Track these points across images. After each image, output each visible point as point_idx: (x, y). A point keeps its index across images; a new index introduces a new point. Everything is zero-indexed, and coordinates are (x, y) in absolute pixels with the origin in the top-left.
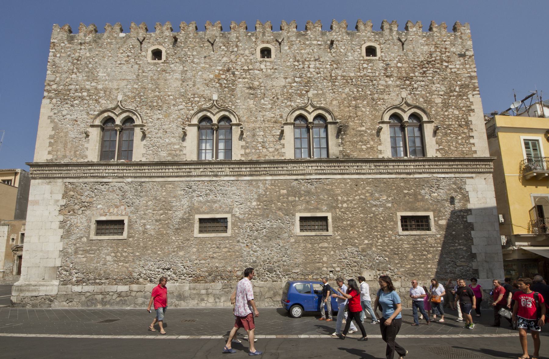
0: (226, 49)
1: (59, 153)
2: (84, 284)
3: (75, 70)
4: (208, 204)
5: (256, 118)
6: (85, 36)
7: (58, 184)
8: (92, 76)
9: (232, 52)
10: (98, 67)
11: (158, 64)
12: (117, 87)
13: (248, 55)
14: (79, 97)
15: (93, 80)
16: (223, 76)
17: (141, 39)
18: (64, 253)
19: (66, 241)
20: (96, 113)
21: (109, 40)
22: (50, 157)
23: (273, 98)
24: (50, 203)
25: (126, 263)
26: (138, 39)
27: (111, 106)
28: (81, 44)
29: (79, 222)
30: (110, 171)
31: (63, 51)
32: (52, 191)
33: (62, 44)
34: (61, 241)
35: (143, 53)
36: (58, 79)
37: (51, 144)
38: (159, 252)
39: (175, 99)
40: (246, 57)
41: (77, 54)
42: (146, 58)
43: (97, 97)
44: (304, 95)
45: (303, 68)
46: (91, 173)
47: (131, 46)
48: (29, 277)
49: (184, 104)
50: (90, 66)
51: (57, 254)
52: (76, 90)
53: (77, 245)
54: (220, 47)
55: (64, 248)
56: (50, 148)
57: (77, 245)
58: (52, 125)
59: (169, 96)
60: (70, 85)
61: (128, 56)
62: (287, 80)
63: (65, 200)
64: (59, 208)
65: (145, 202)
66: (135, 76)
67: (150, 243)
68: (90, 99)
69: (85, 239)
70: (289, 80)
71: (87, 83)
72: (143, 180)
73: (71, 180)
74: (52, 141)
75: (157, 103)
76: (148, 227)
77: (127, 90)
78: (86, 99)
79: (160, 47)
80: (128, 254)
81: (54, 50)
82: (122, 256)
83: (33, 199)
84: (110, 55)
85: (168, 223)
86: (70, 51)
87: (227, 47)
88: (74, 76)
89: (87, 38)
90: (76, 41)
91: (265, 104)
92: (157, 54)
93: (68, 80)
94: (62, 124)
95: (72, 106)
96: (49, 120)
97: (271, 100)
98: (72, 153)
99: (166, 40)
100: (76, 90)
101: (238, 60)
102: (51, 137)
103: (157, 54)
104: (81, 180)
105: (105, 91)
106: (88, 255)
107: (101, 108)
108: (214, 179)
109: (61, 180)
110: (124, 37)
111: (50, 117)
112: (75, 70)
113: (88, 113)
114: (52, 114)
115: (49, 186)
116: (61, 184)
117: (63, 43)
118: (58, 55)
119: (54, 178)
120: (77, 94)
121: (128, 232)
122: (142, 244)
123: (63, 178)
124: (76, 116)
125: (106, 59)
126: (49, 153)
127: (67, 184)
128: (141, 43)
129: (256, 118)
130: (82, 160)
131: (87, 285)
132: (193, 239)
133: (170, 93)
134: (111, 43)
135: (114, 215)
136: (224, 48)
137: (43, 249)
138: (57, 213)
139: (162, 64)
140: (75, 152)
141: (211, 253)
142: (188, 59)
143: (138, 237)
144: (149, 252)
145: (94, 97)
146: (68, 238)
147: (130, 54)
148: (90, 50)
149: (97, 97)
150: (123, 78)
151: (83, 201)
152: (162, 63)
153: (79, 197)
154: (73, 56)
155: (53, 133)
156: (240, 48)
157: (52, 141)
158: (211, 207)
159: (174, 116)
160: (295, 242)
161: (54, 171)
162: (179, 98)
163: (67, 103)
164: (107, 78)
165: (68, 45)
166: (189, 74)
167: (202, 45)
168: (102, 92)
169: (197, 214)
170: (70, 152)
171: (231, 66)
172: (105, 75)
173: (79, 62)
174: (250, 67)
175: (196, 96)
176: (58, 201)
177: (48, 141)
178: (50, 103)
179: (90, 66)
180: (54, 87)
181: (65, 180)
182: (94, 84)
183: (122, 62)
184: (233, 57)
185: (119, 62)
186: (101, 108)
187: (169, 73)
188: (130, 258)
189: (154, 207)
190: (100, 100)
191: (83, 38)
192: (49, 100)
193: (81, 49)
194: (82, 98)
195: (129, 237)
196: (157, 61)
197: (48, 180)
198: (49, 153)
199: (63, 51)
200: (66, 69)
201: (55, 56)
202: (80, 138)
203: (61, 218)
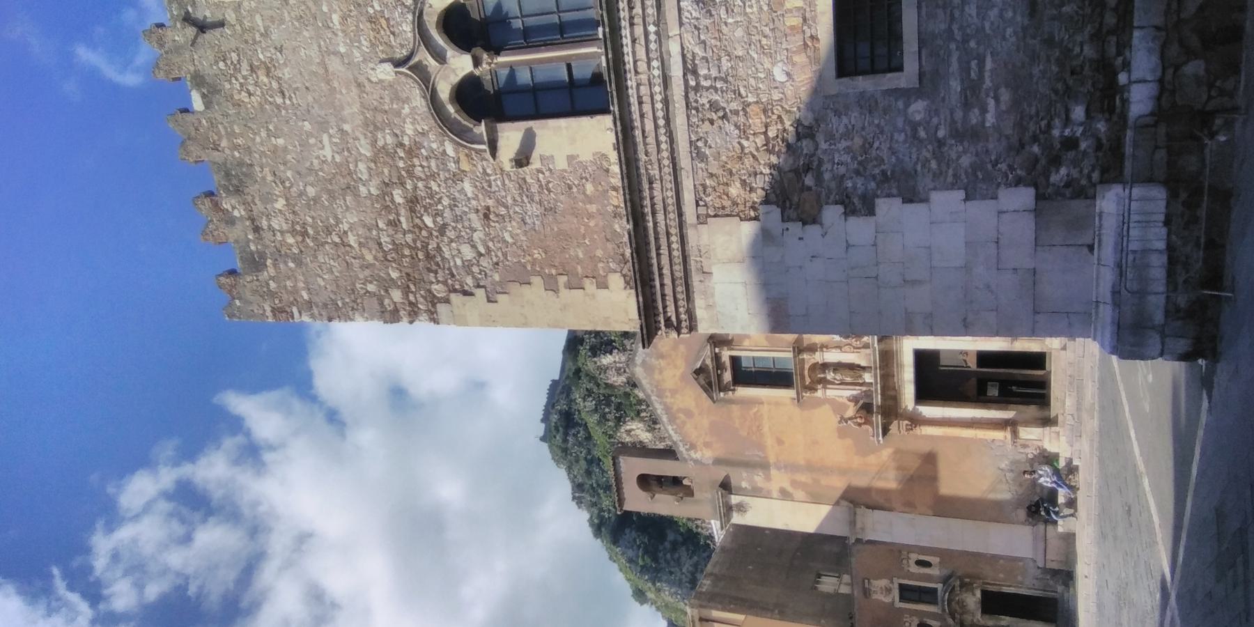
1: (599, 253)
2: (1122, 78)
6: (231, 221)
7: (705, 239)
8: (342, 183)
10: (308, 164)
12: (355, 91)
14: (412, 210)
15: (350, 174)
17: (191, 31)
18: (977, 185)
19: (924, 182)
22: (616, 281)
26: (194, 43)
27: (418, 101)
28: (257, 229)
29: (844, 144)
30: (641, 53)
33: (273, 285)
34: (926, 200)
41: (290, 240)
46: (656, 127)
50: (311, 191)
51: (981, 210)
52: (394, 224)
53: (941, 134)
57: (941, 134)
58: (514, 288)
60: (380, 244)
61: (253, 69)
64: (795, 228)
68: (411, 174)
69: (918, 109)
71: (363, 190)
73: (688, 197)
74: (562, 280)
77: (356, 53)
78: (415, 188)
84: (264, 134)
86: (286, 263)
88: (352, 239)
89: (236, 213)
90: (253, 248)
93: (369, 258)
94: (505, 255)
95: (442, 229)
98: (593, 208)
100: (394, 224)
102: (551, 286)
104: (685, 161)
105: (376, 128)
106: (988, 83)
107: (432, 136)
109: (691, 234)
110: (204, 96)
113: (457, 177)
114: (480, 293)
115: (714, 270)
120: (403, 219)
123: (681, 225)
124: (473, 216)
125: (280, 141)
126: (603, 285)
127: (702, 210)
130: (616, 169)
131: (1127, 66)
134: (231, 135)
138: (813, 230)
140: (589, 200)
145: (401, 164)
148: (268, 198)
150: (321, 71)
151: (760, 140)
153: (748, 162)
155: (537, 280)
161: (664, 262)
163: (439, 249)
165: (272, 271)
170: (590, 216)
172: (325, 138)
173: (311, 231)
177: (564, 292)
178: (447, 301)
179: (311, 191)
180: (397, 295)
185: (279, 100)
186: (432, 136)
191: (239, 226)
192: (438, 305)
194: (413, 202)
197: (695, 279)
198: (603, 285)
199: (289, 283)
202: (541, 186)
203: (832, 213)
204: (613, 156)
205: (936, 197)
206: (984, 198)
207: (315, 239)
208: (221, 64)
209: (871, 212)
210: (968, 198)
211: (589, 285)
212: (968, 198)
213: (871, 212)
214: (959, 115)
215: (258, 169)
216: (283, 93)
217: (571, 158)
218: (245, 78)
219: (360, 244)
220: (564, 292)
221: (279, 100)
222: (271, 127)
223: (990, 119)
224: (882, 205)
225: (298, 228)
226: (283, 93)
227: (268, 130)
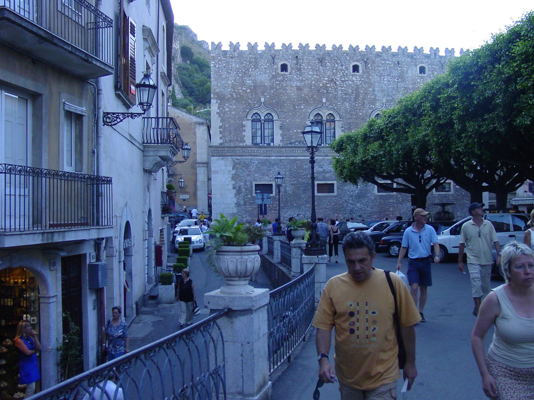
11: (285, 75)
16: (328, 85)
18: (238, 205)
19: (238, 196)
22: (221, 141)
28: (232, 57)
33: (219, 58)
35: (275, 67)
51: (233, 205)
56: (221, 135)
58: (220, 118)
61: (265, 68)
72: (282, 158)
74: (221, 130)
79: (286, 63)
82: (273, 207)
87: (330, 64)
92: (284, 68)
102: (220, 127)
104: (243, 157)
108: (326, 158)
111: (217, 113)
118: (217, 66)
126: (221, 138)
135: (266, 180)
136: (328, 64)
140: (237, 138)
155: (221, 124)
157: (221, 130)
158: (324, 176)
160: (375, 199)
165: (223, 58)
174: (346, 79)
176: (230, 171)
198: (221, 138)
203: (233, 182)
204: (245, 144)
217: (244, 136)
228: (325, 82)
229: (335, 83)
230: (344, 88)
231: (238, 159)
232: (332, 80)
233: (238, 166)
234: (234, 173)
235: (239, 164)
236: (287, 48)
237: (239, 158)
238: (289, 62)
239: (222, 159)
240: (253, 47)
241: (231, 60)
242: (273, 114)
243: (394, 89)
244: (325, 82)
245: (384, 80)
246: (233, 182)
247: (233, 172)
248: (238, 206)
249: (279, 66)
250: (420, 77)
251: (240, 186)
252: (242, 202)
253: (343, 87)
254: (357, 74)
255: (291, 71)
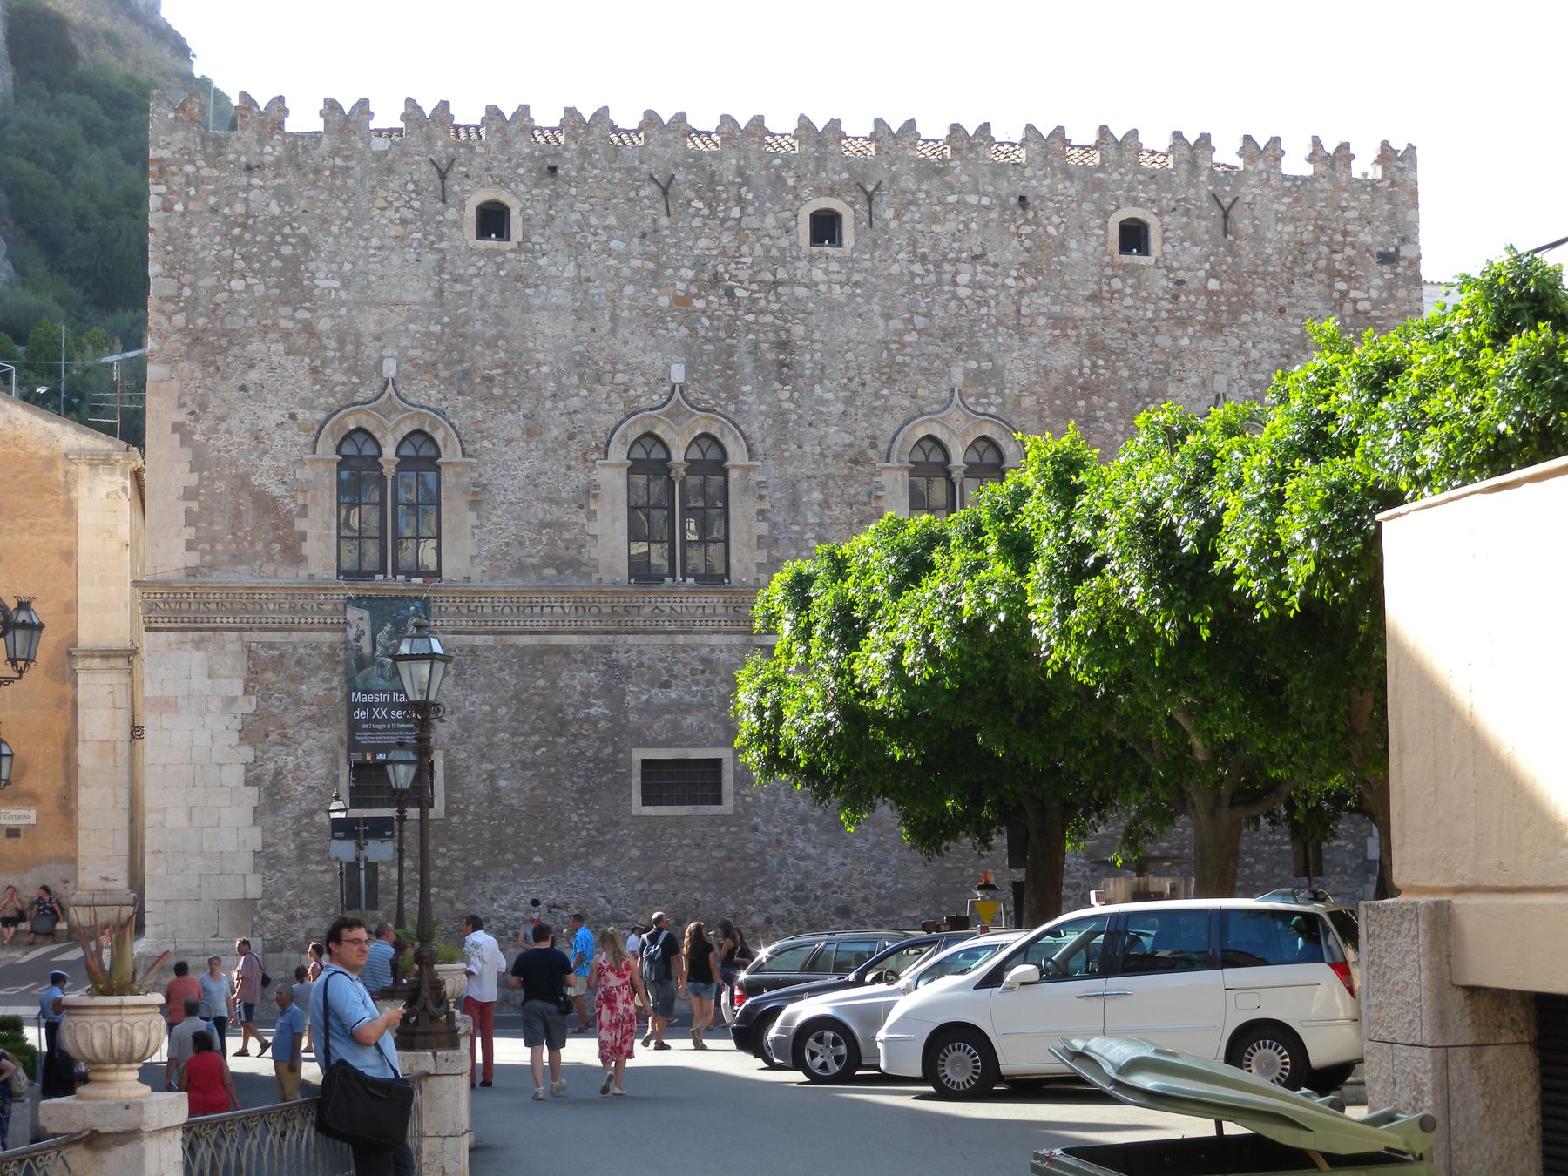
0: (706, 212)
3: (240, 265)
4: (667, 716)
5: (800, 447)
7: (229, 647)
9: (724, 221)
11: (499, 253)
13: (775, 233)
18: (267, 859)
19: (269, 820)
20: (321, 416)
21: (339, 161)
22: (194, 559)
23: (850, 380)
24: (212, 708)
25: (447, 888)
28: (249, 168)
31: (192, 192)
32: (210, 668)
33: (189, 168)
34: (255, 824)
35: (451, 214)
36: (187, 292)
37: (190, 519)
38: (537, 859)
39: (557, 376)
40: (766, 241)
41: (239, 208)
42: (460, 228)
43: (317, 363)
44: (942, 373)
45: (939, 282)
47: (411, 187)
48: (170, 928)
49: (584, 393)
51: (246, 860)
53: (304, 834)
54: (689, 203)
55: (266, 845)
56: (190, 532)
57: (304, 834)
59: (538, 365)
61: (404, 222)
62: (891, 323)
63: (254, 699)
64: (237, 724)
65: (487, 708)
66: (429, 293)
67: (510, 830)
70: (896, 324)
71: (285, 310)
72: (478, 640)
73: (267, 637)
74: (194, 506)
75: (504, 387)
76: (502, 783)
79: (504, 197)
80: (452, 862)
81: (163, 189)
83: (158, 694)
85: (558, 772)
86: (214, 193)
89: (268, 149)
91: (824, 402)
92: (493, 220)
96: (177, 436)
97: (844, 387)
99: (521, 171)
101: (745, 249)
102: (189, 494)
103: (493, 220)
104: (295, 636)
107: (332, 400)
111: (177, 427)
112: (240, 265)
114: (180, 416)
116: (237, 647)
117: (192, 162)
118: (179, 207)
119: (214, 630)
121: (448, 798)
122: (486, 834)
128: (443, 177)
129: (800, 447)
132: (627, 820)
133: (540, 356)
136: (698, 204)
137: (206, 847)
138: (234, 738)
139: (511, 256)
141: (680, 862)
142: (590, 238)
143: (475, 814)
144: (509, 856)
146: (274, 811)
147: (407, 214)
149: (317, 363)
152: (512, 251)
154: (227, 210)
155: (193, 480)
156: (750, 210)
157: (194, 506)
158: (676, 726)
159: (555, 433)
162: (568, 375)
164: (343, 295)
165: (205, 172)
166: (597, 290)
167: (632, 194)
168: (333, 344)
169: (638, 746)
171: (721, 269)
172: (336, 284)
175: (620, 367)
176: (233, 700)
177: (183, 505)
181: (247, 636)
182: (302, 315)
183: (388, 242)
184: (726, 238)
185: (375, 242)
186: (332, 400)
187: (536, 286)
188: (458, 875)
189: (515, 724)
190: (328, 372)
193: (249, 187)
195: (450, 812)
196: (492, 243)
197: (196, 635)
198: (190, 546)
200: (209, 255)
201: (167, 208)
203: (248, 753)
205: (259, 829)
206: (256, 865)
207: (239, 239)
208: (411, 187)
209: (247, 783)
210: (255, 853)
211: (190, 532)
212: (255, 853)
213: (247, 783)
214: (317, 846)
215: (313, 193)
216: (379, 248)
218: (397, 210)
219: (231, 292)
220: (183, 505)
221: (375, 242)
222: (349, 224)
223: (312, 867)
224: (253, 792)
225: (250, 221)
226: (379, 248)
227: (348, 219)
228: (680, 286)
229: (730, 293)
230: (769, 318)
231: (271, 646)
232: (716, 280)
233: (270, 675)
234: (250, 709)
235: (277, 663)
236: (506, 127)
237: (277, 637)
238: (515, 194)
239: (198, 645)
240: (347, 118)
241: (244, 180)
242: (439, 436)
243: (999, 322)
244: (680, 286)
245: (955, 283)
246: (248, 753)
247: (249, 705)
248: (270, 867)
249: (471, 214)
250: (1124, 267)
251: (278, 773)
252: (287, 849)
253: (762, 312)
254: (830, 251)
255: (526, 237)
